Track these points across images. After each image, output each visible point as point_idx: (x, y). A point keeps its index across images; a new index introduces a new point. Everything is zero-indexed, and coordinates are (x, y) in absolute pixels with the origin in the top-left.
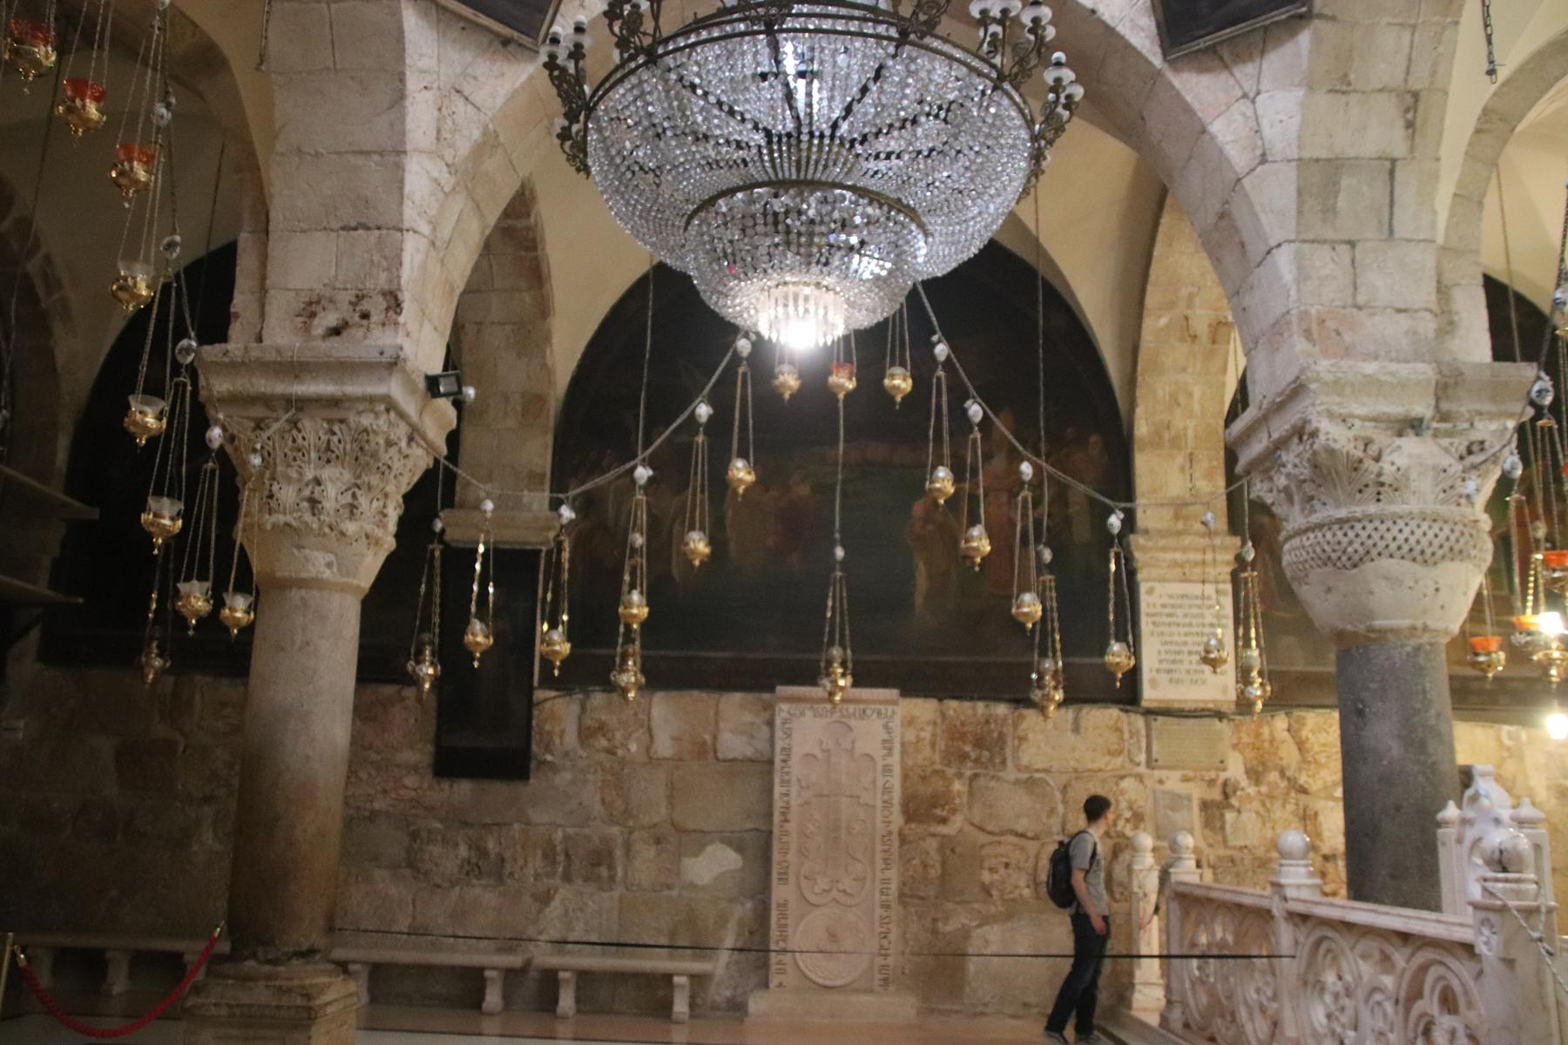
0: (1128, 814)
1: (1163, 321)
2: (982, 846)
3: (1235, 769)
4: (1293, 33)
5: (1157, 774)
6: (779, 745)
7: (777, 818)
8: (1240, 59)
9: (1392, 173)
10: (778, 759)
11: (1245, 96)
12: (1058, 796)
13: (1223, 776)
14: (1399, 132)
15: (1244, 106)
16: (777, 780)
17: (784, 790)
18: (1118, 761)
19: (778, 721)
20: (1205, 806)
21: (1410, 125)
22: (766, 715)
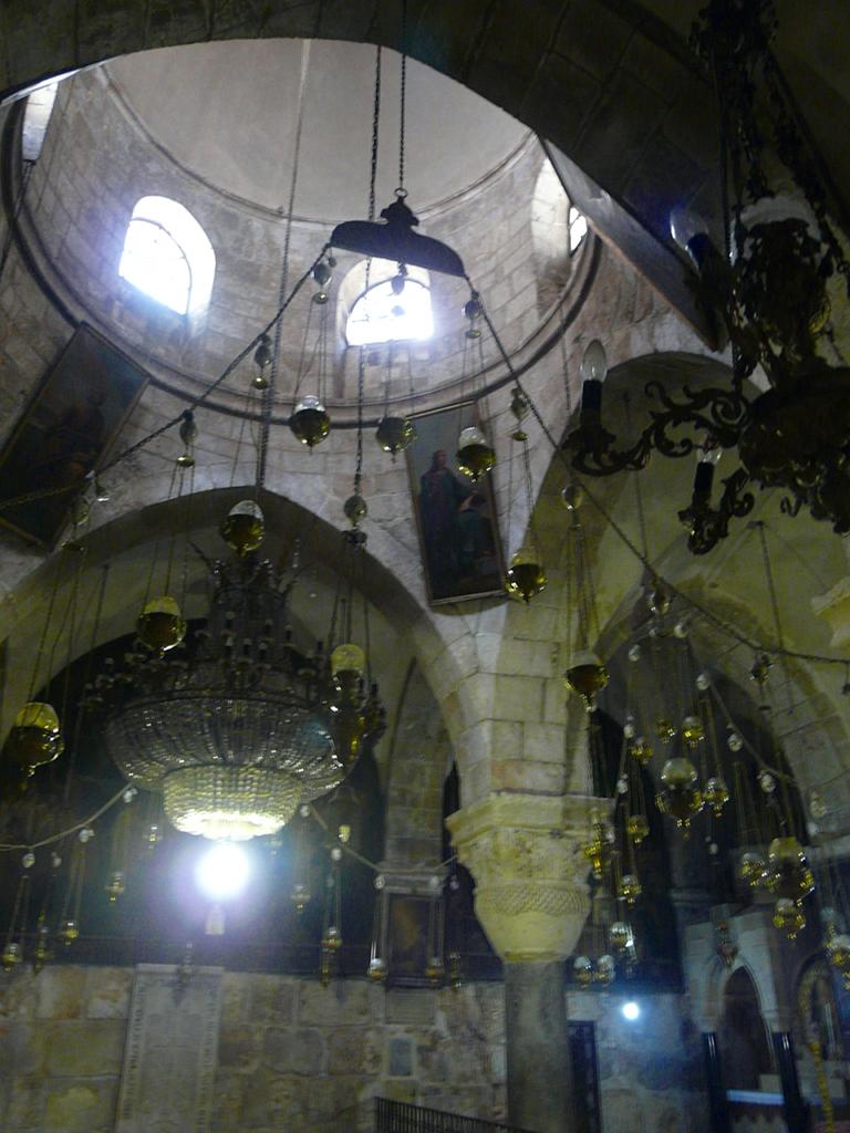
0: (370, 1057)
1: (410, 727)
2: (272, 1082)
3: (441, 1024)
4: (497, 605)
5: (392, 1026)
6: (136, 1008)
7: (127, 1064)
8: (470, 611)
9: (544, 685)
10: (134, 1017)
11: (469, 633)
12: (325, 1043)
13: (433, 1028)
14: (548, 664)
15: (469, 639)
16: (131, 1035)
17: (134, 1043)
18: (364, 1019)
19: (136, 990)
20: (421, 1049)
21: (555, 660)
22: (126, 984)
